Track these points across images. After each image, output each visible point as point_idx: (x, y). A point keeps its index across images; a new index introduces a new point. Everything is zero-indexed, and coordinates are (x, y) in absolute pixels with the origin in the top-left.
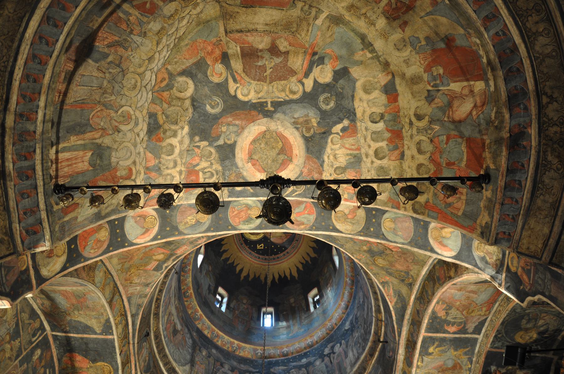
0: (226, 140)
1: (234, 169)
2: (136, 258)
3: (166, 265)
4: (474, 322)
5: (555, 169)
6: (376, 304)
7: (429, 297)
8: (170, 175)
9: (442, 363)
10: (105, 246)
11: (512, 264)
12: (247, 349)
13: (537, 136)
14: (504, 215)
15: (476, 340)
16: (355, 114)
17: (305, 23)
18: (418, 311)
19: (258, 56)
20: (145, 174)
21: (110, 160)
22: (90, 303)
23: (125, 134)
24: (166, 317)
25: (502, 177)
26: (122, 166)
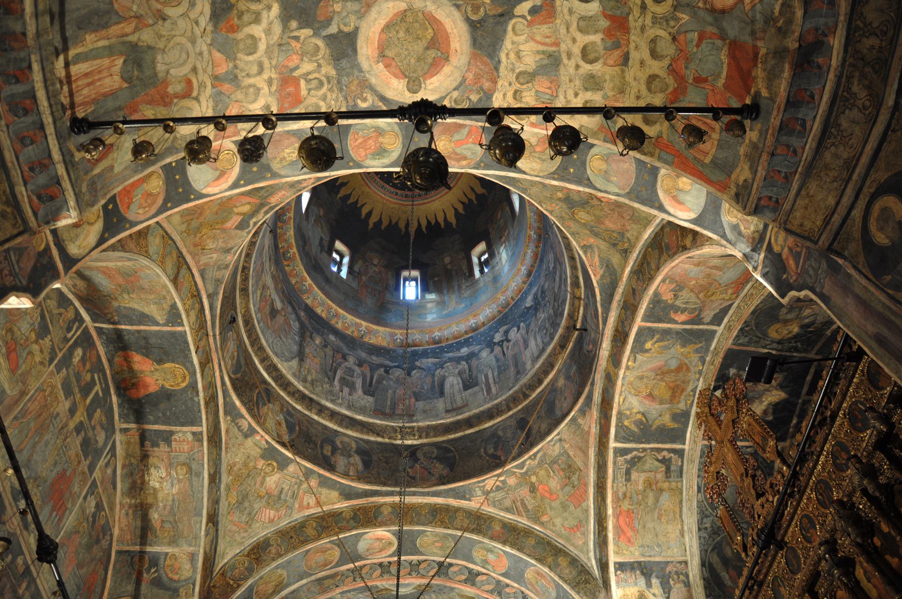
0: (342, 27)
1: (356, 73)
2: (208, 212)
3: (254, 220)
4: (714, 309)
5: (861, 106)
6: (572, 274)
7: (652, 273)
8: (254, 86)
9: (663, 363)
10: (160, 202)
11: (776, 240)
12: (380, 334)
13: (842, 51)
14: (774, 171)
15: (715, 332)
18: (634, 290)
20: (213, 87)
21: (154, 68)
22: (145, 283)
23: (175, 23)
24: (259, 292)
25: (778, 112)
26: (175, 77)
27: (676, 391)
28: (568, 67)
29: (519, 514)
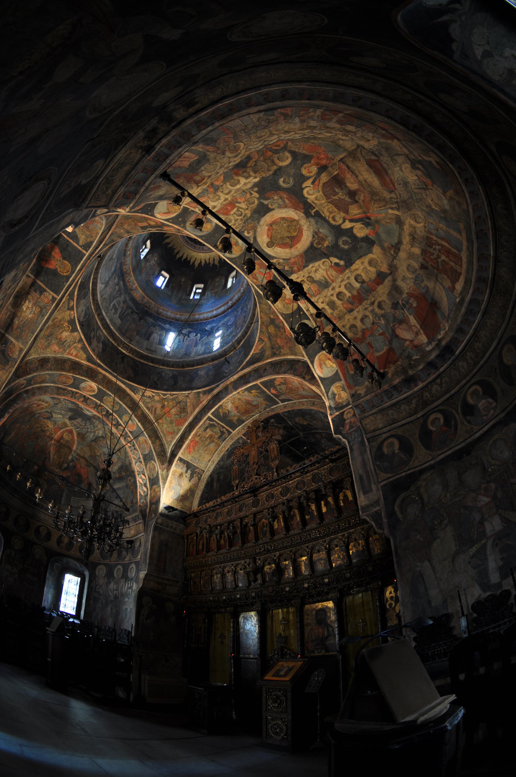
0: (270, 204)
15: (279, 403)
16: (351, 265)
17: (384, 203)
19: (341, 186)
27: (247, 412)
28: (329, 292)
29: (151, 413)
